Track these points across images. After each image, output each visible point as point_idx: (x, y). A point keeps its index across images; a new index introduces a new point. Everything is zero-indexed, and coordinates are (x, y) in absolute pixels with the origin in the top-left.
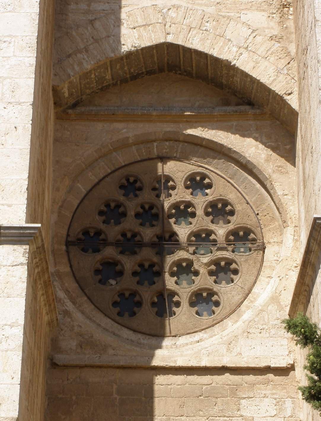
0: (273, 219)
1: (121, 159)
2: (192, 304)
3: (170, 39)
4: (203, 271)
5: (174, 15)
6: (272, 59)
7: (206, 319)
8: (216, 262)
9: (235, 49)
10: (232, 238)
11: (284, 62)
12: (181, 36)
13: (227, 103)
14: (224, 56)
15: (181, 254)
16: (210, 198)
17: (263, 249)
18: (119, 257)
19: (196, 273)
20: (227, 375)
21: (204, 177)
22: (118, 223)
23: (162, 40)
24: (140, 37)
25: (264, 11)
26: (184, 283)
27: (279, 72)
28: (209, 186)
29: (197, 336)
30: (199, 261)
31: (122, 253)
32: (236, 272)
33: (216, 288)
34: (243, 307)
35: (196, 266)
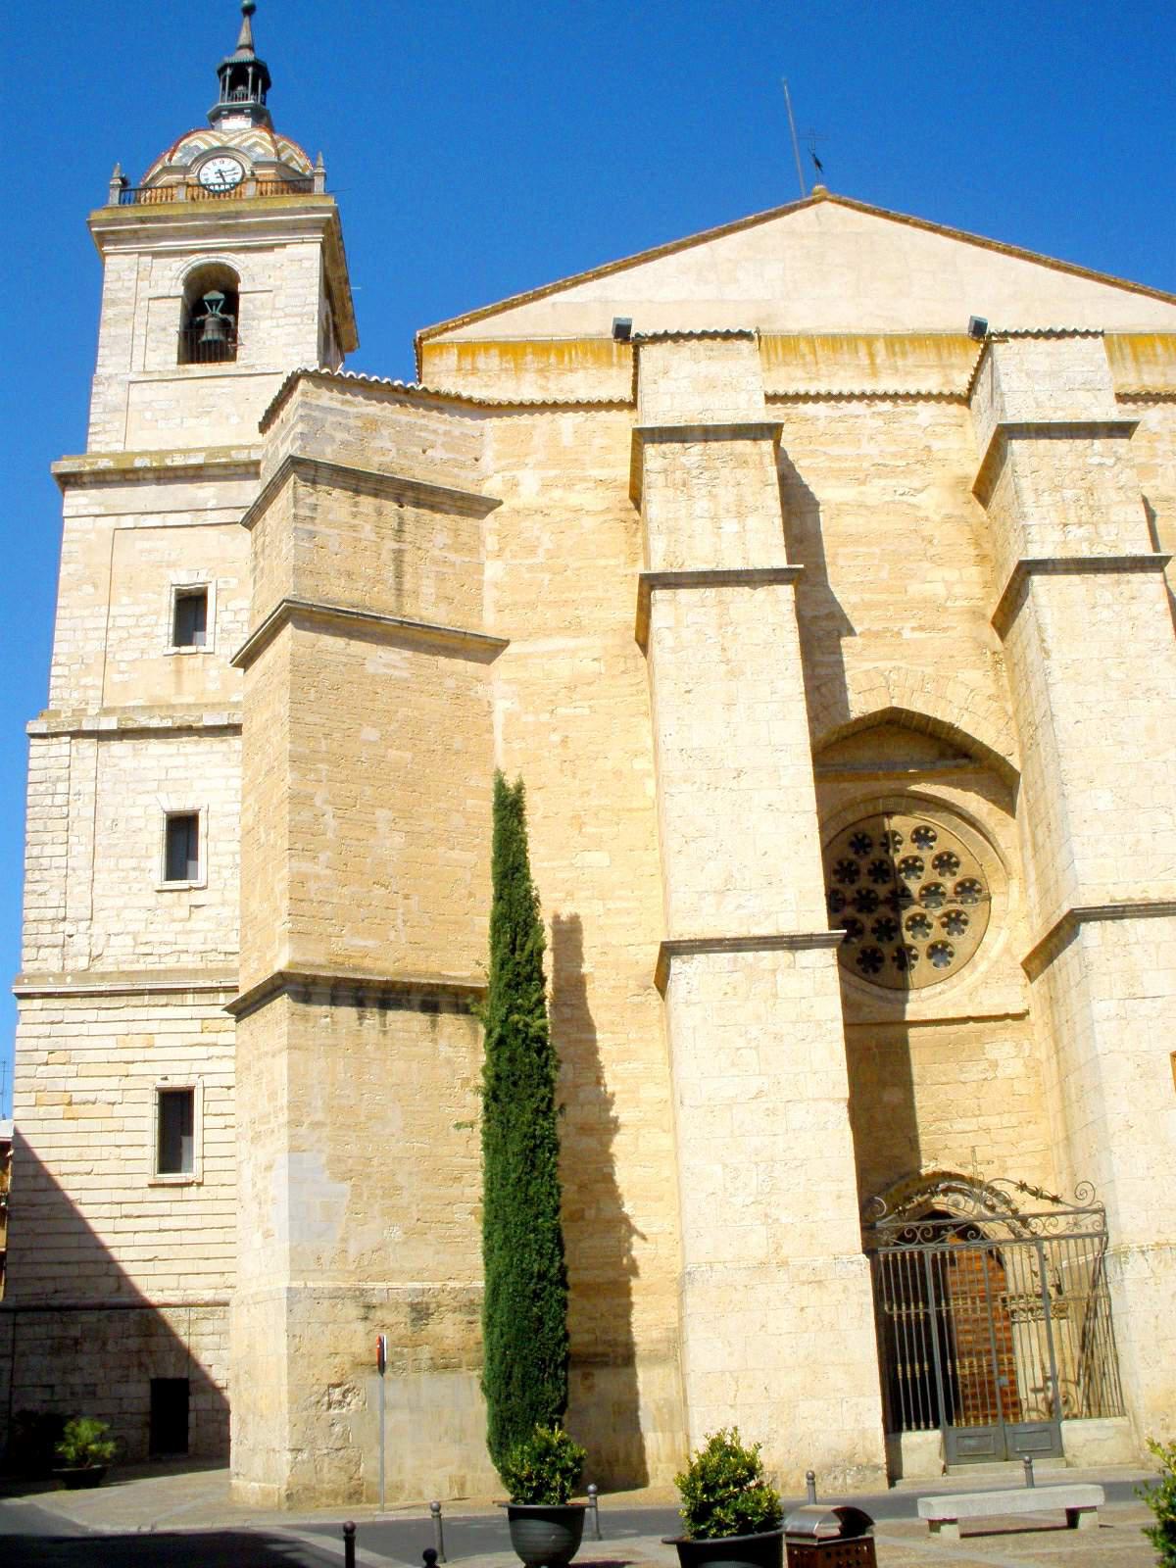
0: (997, 870)
1: (850, 818)
2: (930, 956)
3: (895, 703)
4: (936, 924)
5: (895, 677)
6: (992, 719)
7: (943, 970)
8: (947, 915)
9: (957, 711)
10: (959, 889)
11: (1002, 722)
12: (905, 700)
13: (942, 756)
14: (947, 719)
15: (915, 909)
16: (936, 852)
17: (990, 899)
18: (858, 916)
19: (930, 926)
20: (971, 1023)
21: (927, 830)
22: (852, 882)
23: (888, 705)
24: (867, 703)
25: (979, 669)
26: (920, 937)
27: (999, 732)
28: (934, 839)
29: (940, 987)
30: (931, 913)
31: (860, 911)
32: (965, 922)
33: (950, 939)
34: (977, 957)
35: (929, 919)
